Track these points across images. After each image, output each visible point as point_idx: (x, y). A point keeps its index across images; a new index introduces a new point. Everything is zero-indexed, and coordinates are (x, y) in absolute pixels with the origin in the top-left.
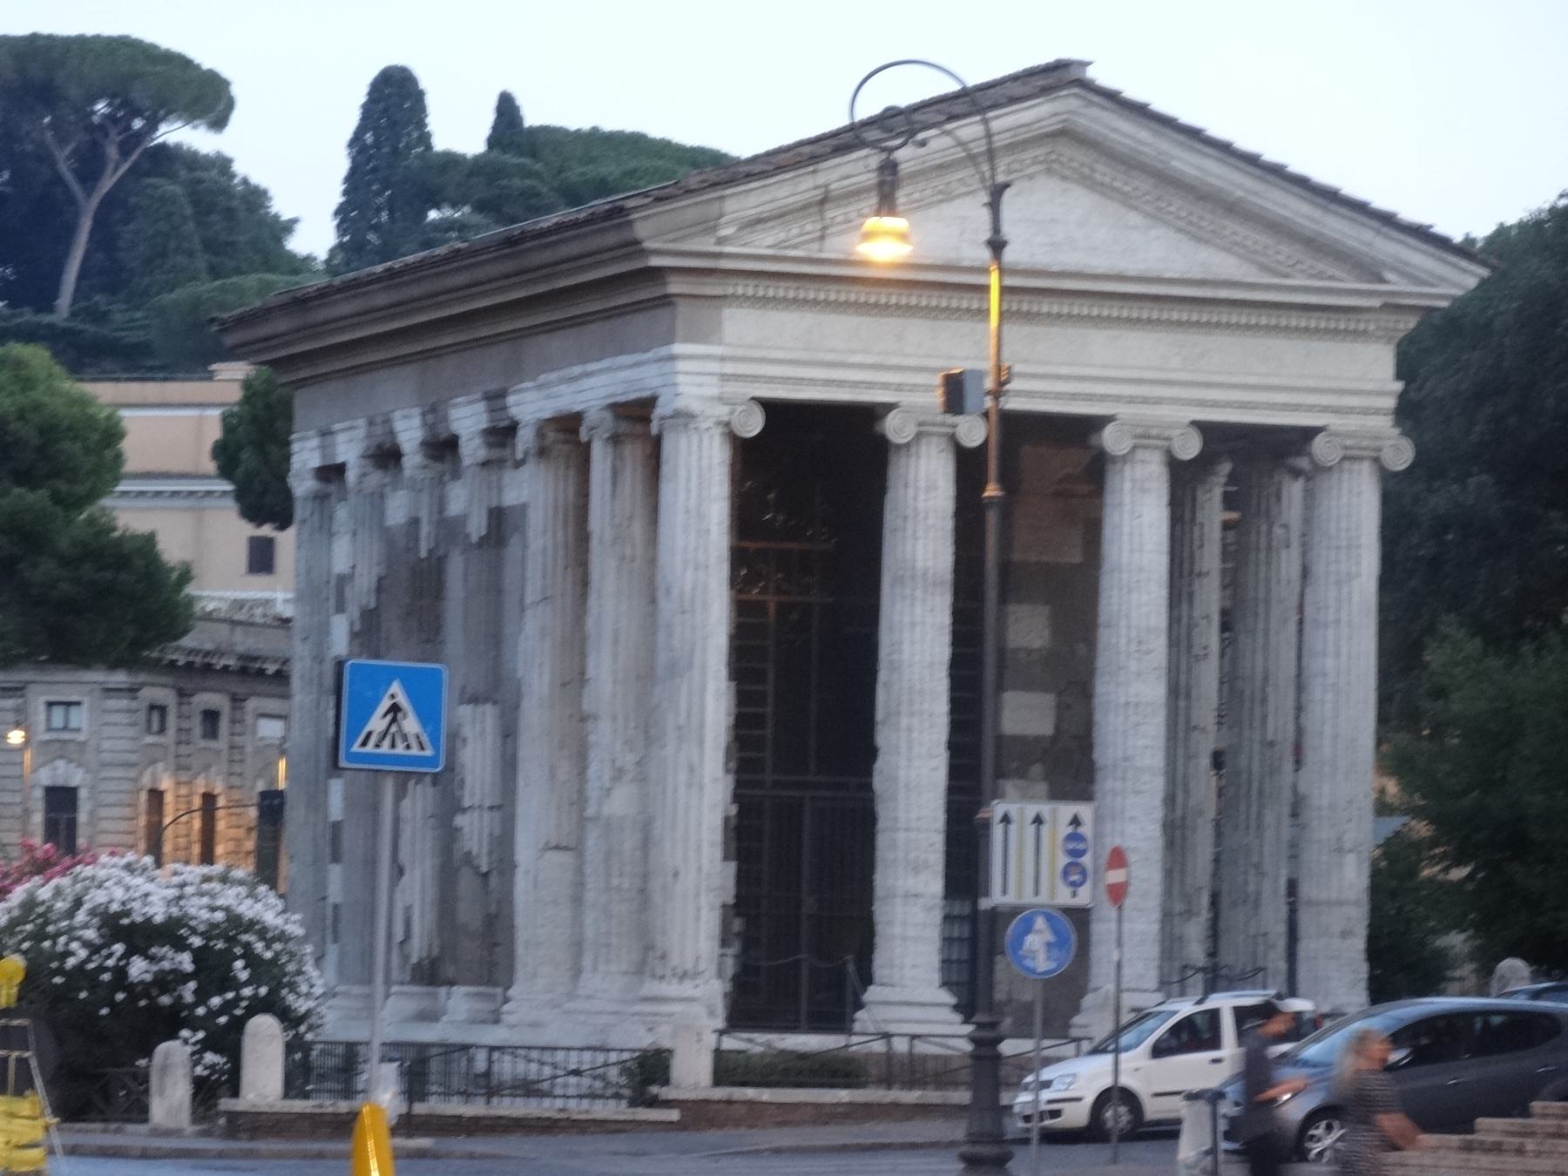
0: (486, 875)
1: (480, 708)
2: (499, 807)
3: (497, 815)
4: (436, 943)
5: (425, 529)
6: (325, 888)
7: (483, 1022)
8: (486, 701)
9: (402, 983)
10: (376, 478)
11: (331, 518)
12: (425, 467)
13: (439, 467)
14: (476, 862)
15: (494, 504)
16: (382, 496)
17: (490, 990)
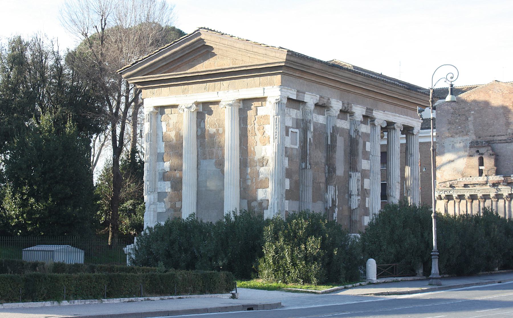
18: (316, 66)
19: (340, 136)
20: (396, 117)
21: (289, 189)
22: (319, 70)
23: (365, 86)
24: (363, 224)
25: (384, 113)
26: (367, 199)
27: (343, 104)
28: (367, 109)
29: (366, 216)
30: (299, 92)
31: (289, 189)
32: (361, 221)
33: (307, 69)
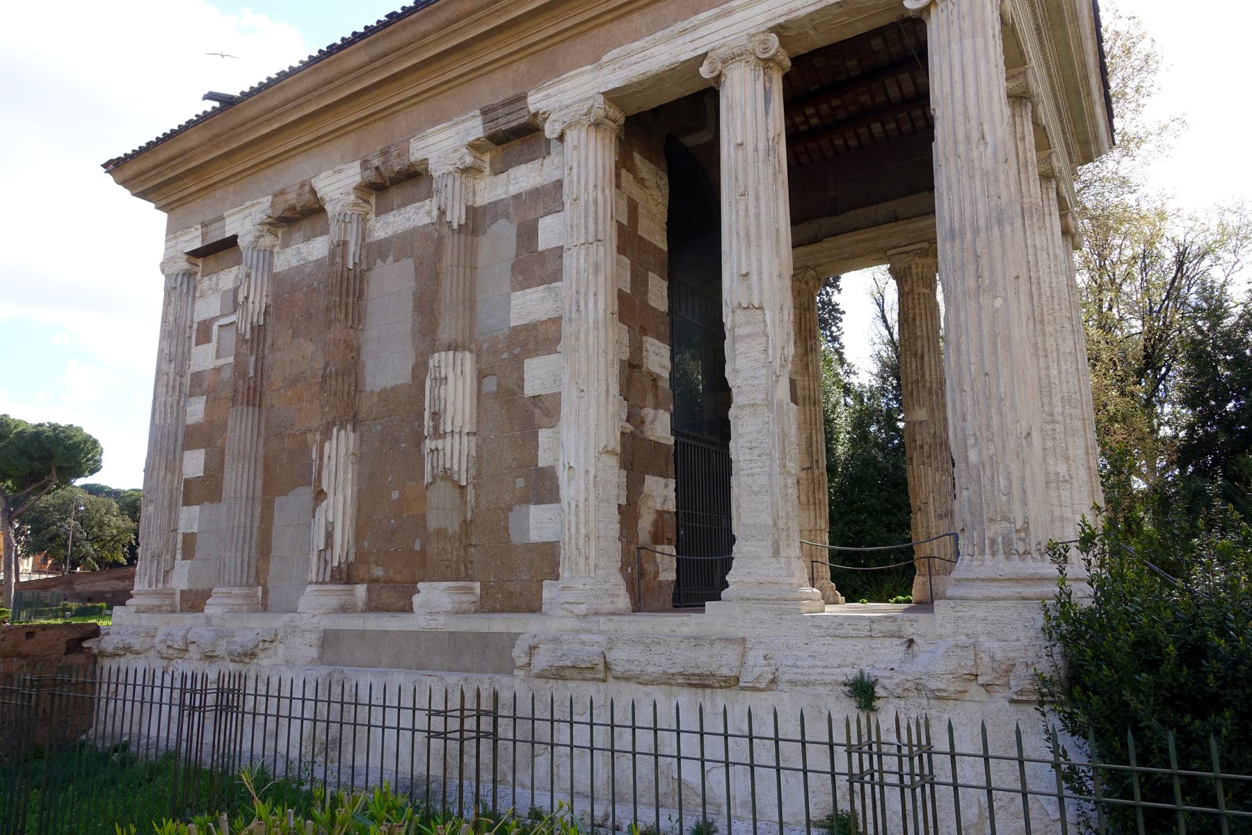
0: (462, 488)
1: (459, 355)
2: (474, 434)
3: (473, 439)
4: (352, 551)
5: (352, 248)
6: (176, 523)
7: (465, 612)
8: (464, 350)
9: (323, 583)
10: (268, 240)
11: (195, 288)
12: (355, 204)
13: (367, 207)
14: (456, 477)
15: (470, 203)
16: (271, 253)
17: (469, 584)
18: (193, 139)
19: (397, 260)
20: (702, 31)
21: (202, 474)
22: (213, 141)
23: (408, 55)
24: (516, 539)
25: (601, 66)
26: (544, 435)
27: (365, 164)
28: (484, 112)
29: (540, 501)
30: (207, 226)
31: (202, 474)
32: (506, 528)
33: (187, 161)
